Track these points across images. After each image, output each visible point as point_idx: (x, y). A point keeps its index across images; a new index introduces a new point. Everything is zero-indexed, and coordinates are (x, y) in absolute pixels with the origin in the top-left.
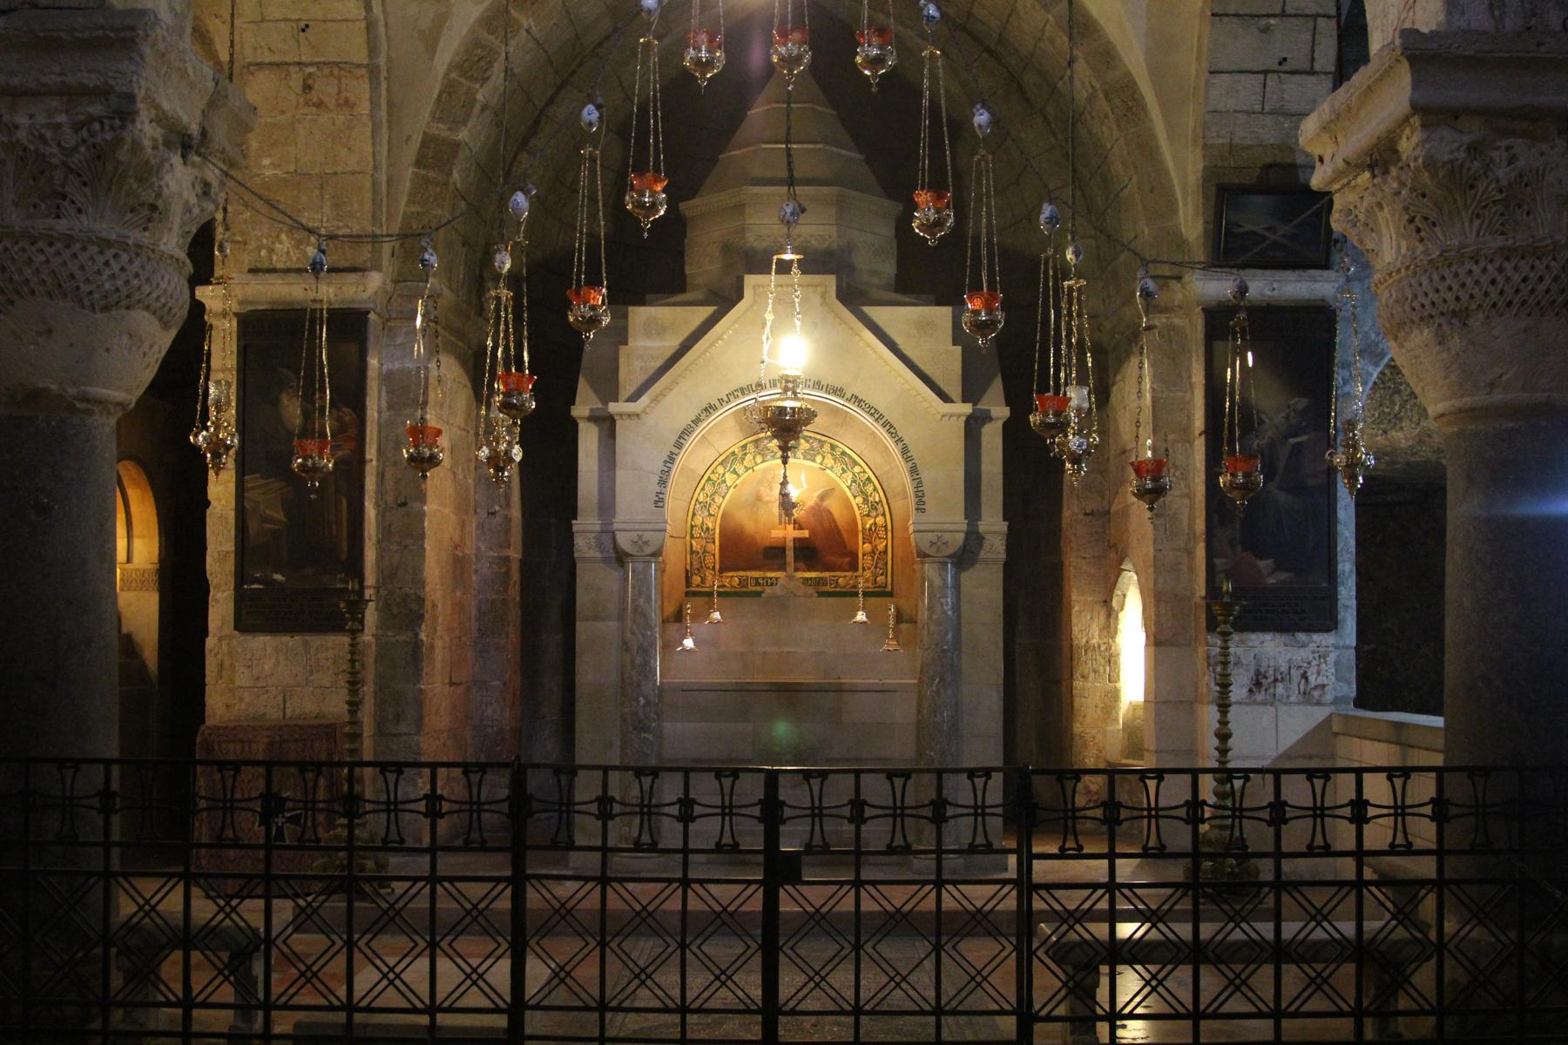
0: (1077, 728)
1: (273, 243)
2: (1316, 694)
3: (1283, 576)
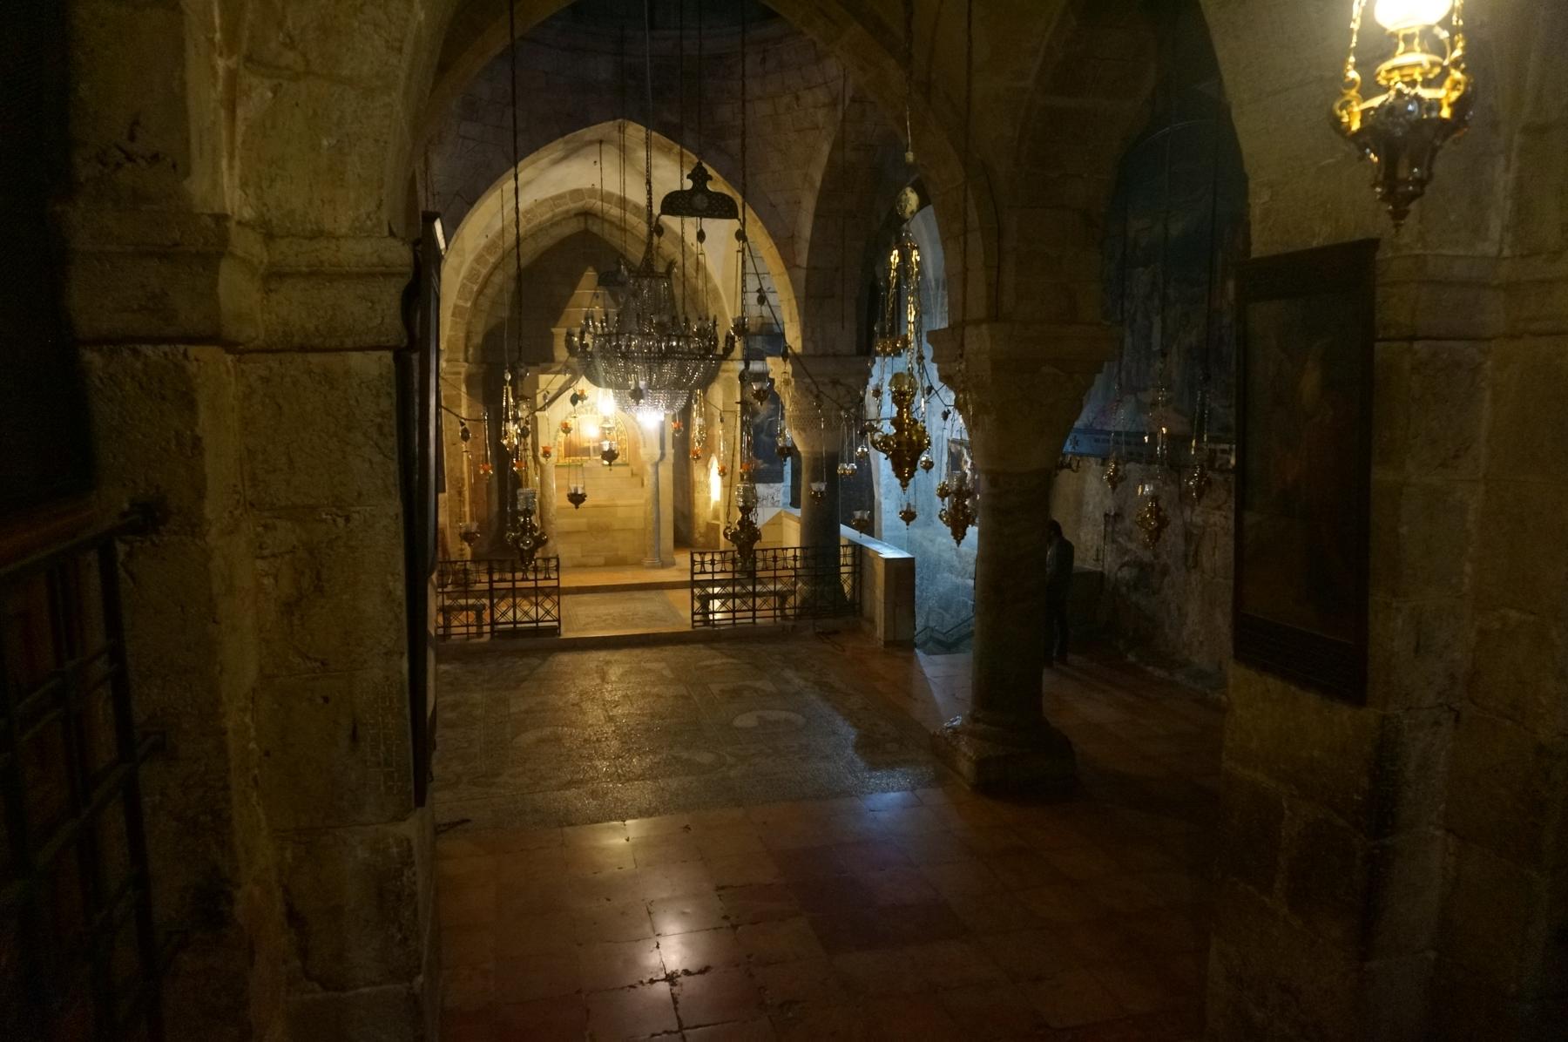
0: (696, 511)
2: (777, 504)
3: (766, 465)
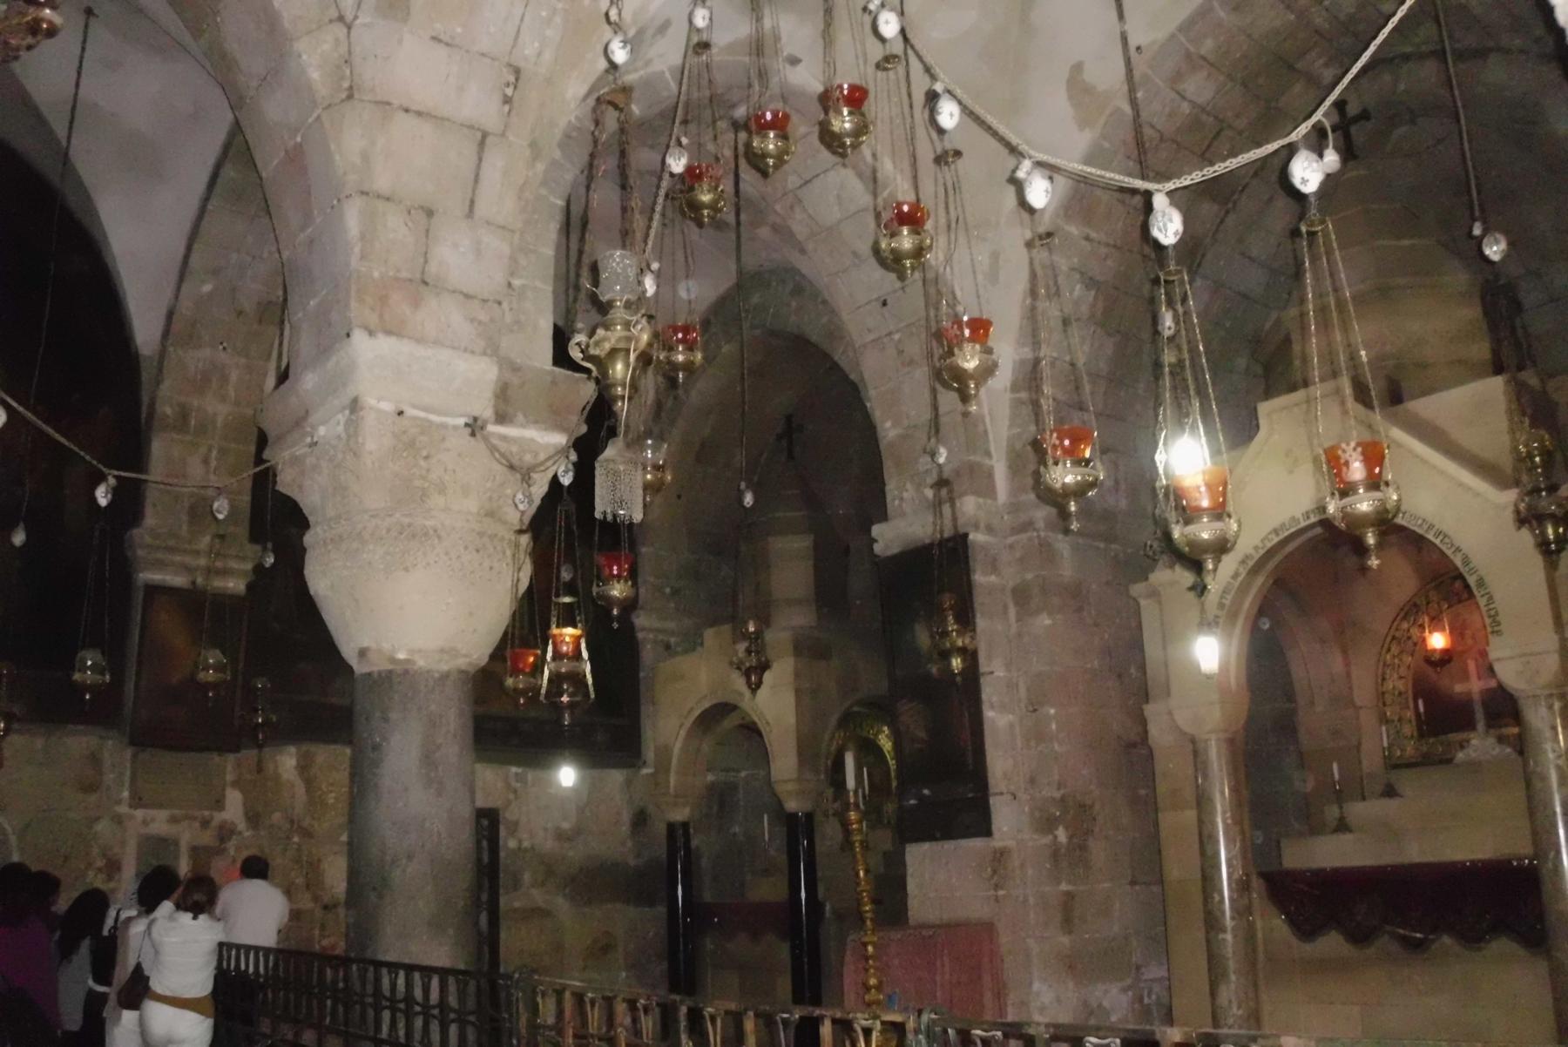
1: (901, 493)
